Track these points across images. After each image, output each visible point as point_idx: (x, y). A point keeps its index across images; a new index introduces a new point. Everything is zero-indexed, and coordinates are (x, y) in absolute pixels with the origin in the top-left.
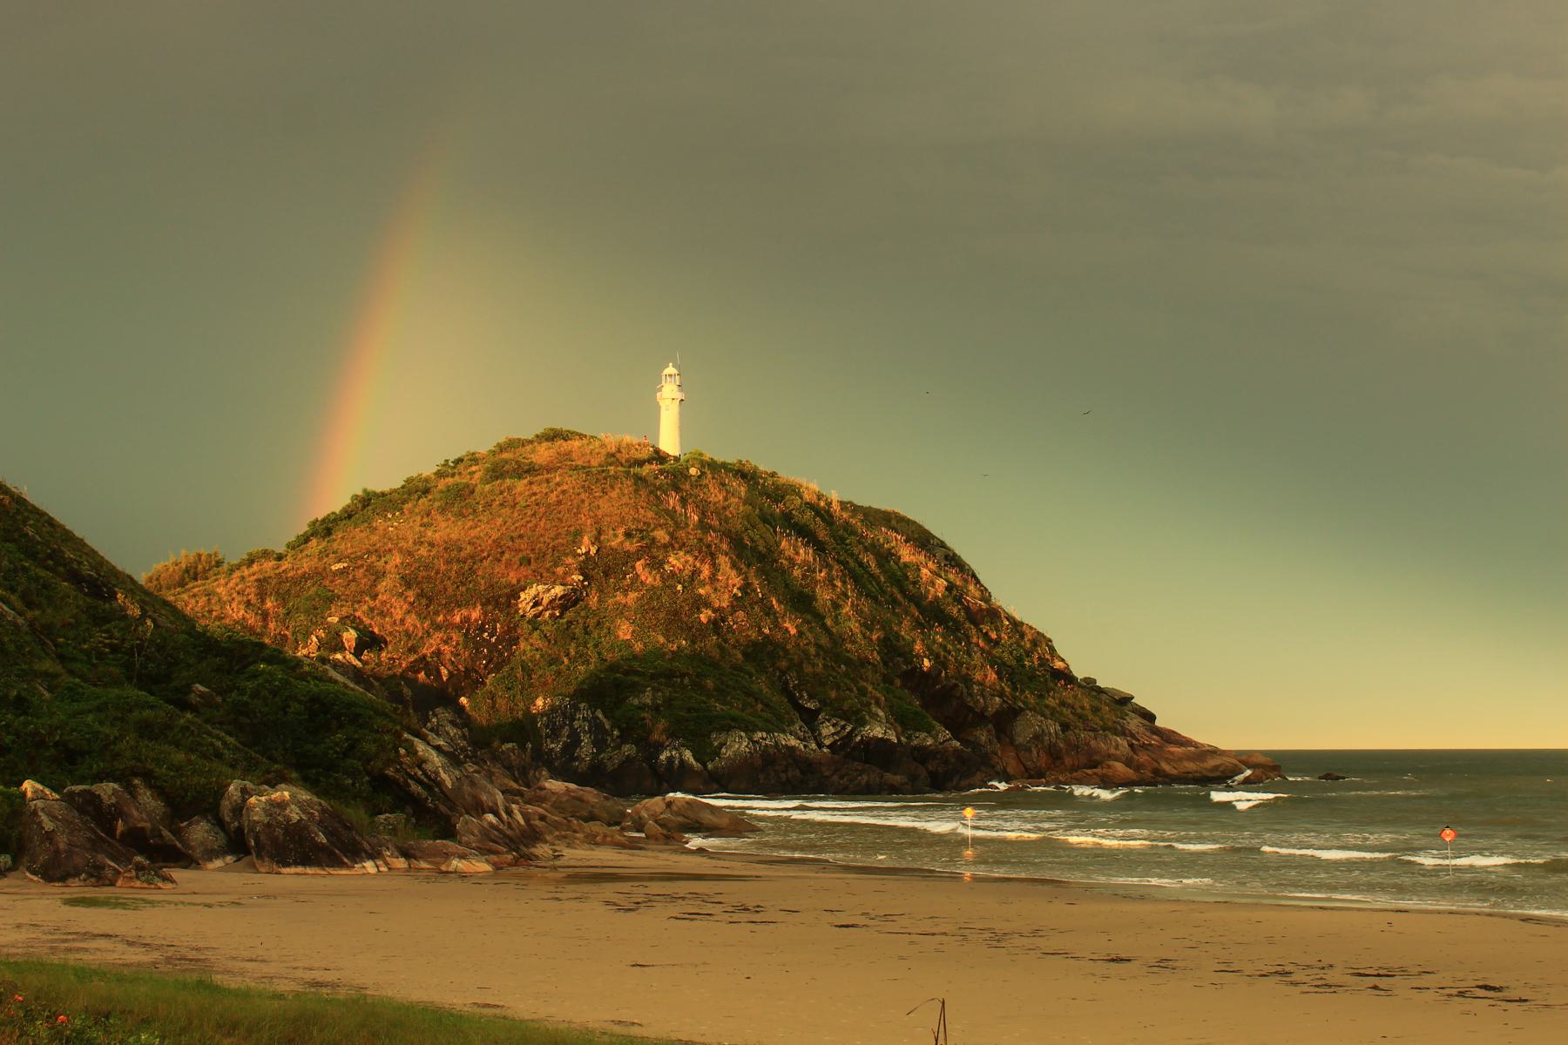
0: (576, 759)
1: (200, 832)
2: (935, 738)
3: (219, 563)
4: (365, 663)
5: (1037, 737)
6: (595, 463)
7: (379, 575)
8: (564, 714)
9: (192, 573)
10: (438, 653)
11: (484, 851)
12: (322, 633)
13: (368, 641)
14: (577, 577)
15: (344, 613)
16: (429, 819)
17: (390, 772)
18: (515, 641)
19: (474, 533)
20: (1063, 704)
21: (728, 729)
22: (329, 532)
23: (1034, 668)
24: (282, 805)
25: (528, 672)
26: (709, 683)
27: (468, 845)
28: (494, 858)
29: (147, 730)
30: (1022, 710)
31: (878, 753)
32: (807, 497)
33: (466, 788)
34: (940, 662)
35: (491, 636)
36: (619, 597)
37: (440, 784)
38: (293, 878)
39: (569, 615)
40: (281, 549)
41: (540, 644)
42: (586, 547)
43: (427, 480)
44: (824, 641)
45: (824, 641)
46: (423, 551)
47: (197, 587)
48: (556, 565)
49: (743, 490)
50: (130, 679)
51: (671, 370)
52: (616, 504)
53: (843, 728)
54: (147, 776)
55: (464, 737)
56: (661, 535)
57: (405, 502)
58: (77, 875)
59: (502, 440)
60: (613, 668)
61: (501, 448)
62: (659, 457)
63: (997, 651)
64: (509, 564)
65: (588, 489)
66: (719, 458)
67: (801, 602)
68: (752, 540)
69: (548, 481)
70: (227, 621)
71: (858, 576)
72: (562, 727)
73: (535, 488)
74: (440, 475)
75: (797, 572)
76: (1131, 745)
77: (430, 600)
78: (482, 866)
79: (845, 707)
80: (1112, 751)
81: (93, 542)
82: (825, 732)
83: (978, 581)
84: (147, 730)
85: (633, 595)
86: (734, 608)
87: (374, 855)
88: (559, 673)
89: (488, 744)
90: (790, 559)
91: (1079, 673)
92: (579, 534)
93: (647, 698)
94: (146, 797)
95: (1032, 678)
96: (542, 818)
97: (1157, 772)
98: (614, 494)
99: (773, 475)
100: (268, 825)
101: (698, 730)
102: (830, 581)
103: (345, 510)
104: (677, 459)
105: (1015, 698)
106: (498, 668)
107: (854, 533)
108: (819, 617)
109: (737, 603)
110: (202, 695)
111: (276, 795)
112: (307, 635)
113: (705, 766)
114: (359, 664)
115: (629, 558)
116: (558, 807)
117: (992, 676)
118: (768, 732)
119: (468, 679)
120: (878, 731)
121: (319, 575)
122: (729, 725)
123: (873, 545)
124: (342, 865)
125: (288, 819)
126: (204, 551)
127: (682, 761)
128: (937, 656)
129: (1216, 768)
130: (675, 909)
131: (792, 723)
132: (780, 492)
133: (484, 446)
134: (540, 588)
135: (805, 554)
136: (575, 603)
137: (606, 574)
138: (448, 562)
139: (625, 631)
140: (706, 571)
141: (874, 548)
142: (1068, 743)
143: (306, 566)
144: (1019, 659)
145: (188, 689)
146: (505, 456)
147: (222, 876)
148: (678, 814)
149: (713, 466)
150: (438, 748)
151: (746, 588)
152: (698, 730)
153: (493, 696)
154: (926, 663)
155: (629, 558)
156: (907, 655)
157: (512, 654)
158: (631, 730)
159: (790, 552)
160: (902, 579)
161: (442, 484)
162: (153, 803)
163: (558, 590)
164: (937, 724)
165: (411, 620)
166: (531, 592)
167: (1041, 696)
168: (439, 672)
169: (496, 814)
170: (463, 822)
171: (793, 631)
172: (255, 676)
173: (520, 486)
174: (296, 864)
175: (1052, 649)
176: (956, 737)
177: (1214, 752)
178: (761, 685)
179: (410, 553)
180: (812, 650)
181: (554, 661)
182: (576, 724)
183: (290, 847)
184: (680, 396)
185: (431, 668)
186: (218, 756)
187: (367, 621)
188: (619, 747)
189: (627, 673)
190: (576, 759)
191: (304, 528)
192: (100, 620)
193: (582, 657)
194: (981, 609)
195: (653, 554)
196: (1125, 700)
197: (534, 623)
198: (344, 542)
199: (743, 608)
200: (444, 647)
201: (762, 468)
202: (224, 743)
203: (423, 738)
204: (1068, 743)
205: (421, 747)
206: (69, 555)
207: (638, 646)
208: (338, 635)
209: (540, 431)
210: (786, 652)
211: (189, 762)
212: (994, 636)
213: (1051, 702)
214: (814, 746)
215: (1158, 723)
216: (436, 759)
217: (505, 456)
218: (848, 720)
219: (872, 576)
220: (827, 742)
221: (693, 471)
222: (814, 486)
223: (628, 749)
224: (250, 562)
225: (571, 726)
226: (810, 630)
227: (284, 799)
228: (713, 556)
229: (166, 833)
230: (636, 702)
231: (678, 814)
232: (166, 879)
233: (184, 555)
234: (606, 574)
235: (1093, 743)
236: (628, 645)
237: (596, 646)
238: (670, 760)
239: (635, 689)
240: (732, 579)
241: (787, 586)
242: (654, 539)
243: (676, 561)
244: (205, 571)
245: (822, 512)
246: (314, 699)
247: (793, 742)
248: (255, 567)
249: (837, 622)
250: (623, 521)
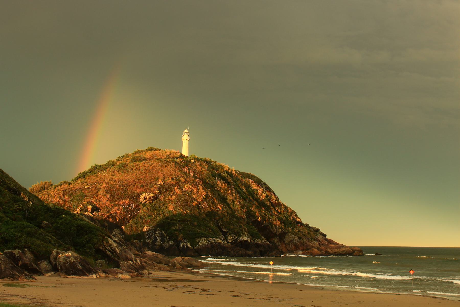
0: (156, 245)
1: (44, 265)
2: (262, 241)
3: (52, 185)
4: (94, 215)
5: (292, 241)
6: (163, 158)
7: (99, 189)
8: (152, 232)
9: (43, 188)
10: (116, 213)
11: (128, 272)
12: (81, 206)
13: (95, 209)
14: (157, 191)
15: (88, 200)
16: (112, 262)
17: (101, 248)
18: (139, 210)
19: (127, 178)
20: (299, 231)
21: (200, 237)
22: (84, 176)
23: (291, 221)
24: (69, 257)
25: (142, 219)
26: (196, 223)
27: (123, 270)
28: (131, 274)
29: (29, 234)
30: (287, 233)
31: (244, 245)
32: (225, 169)
33: (123, 253)
34: (264, 218)
35: (132, 208)
36: (170, 197)
37: (116, 252)
38: (72, 279)
39: (155, 202)
40: (70, 181)
41: (146, 211)
42: (160, 182)
43: (114, 162)
44: (230, 211)
45: (230, 211)
46: (112, 183)
47: (45, 192)
48: (151, 188)
49: (207, 167)
50: (24, 219)
51: (186, 131)
52: (170, 170)
53: (235, 237)
54: (29, 248)
55: (123, 238)
56: (182, 179)
57: (107, 168)
58: (7, 277)
59: (136, 150)
60: (167, 218)
61: (136, 153)
62: (182, 156)
63: (280, 215)
64: (137, 187)
65: (161, 165)
66: (200, 157)
67: (223, 200)
68: (209, 181)
69: (149, 163)
70: (54, 202)
71: (240, 192)
72: (152, 235)
73: (145, 165)
74: (118, 160)
75: (222, 191)
76: (319, 244)
77: (114, 197)
78: (127, 276)
79: (236, 231)
80: (314, 245)
81: (14, 178)
82: (229, 238)
83: (275, 195)
84: (29, 234)
85: (173, 197)
86: (203, 201)
87: (96, 273)
88: (151, 219)
89: (130, 240)
90: (220, 187)
91: (304, 222)
92: (158, 178)
93: (177, 227)
94: (28, 254)
95: (290, 223)
96: (146, 262)
97: (327, 252)
98: (169, 167)
99: (215, 162)
100: (64, 263)
101: (192, 237)
102: (232, 194)
103: (89, 170)
104: (187, 157)
105: (285, 229)
106: (133, 218)
107: (239, 180)
108: (228, 205)
109: (204, 200)
110: (46, 224)
111: (67, 254)
112: (77, 207)
113: (194, 248)
114: (92, 216)
115: (173, 186)
116: (150, 259)
117: (279, 223)
118: (213, 238)
119: (124, 221)
120: (245, 238)
121: (81, 189)
122: (201, 236)
123: (244, 184)
124: (86, 275)
125: (70, 261)
126: (47, 182)
127: (187, 246)
128: (263, 217)
129: (344, 251)
130: (185, 290)
131: (220, 235)
132: (217, 167)
133: (130, 153)
134: (146, 194)
135: (224, 186)
136: (156, 199)
137: (166, 191)
138: (119, 186)
139: (171, 207)
140: (195, 190)
141: (245, 184)
142: (300, 242)
143: (77, 186)
144: (287, 218)
145: (42, 222)
146: (137, 155)
147: (50, 278)
148: (185, 262)
149: (198, 159)
150: (115, 241)
151: (207, 195)
152: (192, 237)
153: (131, 226)
154: (259, 218)
155: (173, 186)
156: (254, 216)
157: (138, 213)
158: (172, 237)
159: (220, 185)
160: (252, 193)
161: (118, 163)
162: (30, 256)
163: (152, 195)
164: (263, 237)
165: (108, 203)
167: (293, 229)
168: (116, 218)
169: (132, 261)
170: (123, 263)
171: (220, 208)
172: (62, 219)
173: (141, 164)
174: (72, 275)
175: (296, 215)
176: (268, 240)
177: (343, 246)
178: (211, 224)
179: (108, 183)
180: (226, 214)
181: (150, 216)
182: (156, 235)
183: (71, 270)
184: (189, 138)
185: (114, 218)
186: (50, 242)
187: (95, 203)
188: (168, 242)
189: (171, 220)
190: (156, 245)
191: (77, 175)
192: (16, 201)
193: (158, 215)
194: (276, 203)
196: (318, 230)
197: (144, 204)
198: (88, 179)
199: (206, 201)
200: (118, 211)
201: (212, 160)
202: (52, 238)
203: (111, 238)
204: (300, 242)
205: (110, 241)
206: (7, 182)
207: (175, 212)
208: (86, 207)
209: (147, 148)
210: (218, 214)
211: (41, 244)
212: (279, 211)
213: (296, 231)
214: (226, 242)
215: (327, 237)
216: (115, 244)
217: (137, 155)
218: (236, 235)
219: (244, 193)
220: (230, 241)
221: (192, 161)
222: (228, 166)
223: (171, 242)
224: (61, 185)
225: (154, 235)
226: (226, 208)
227: (69, 255)
228: (197, 185)
229: (34, 265)
230: (174, 228)
231: (185, 262)
232: (34, 279)
233: (41, 183)
234: (166, 191)
235: (308, 243)
236: (172, 211)
237: (162, 212)
238: (184, 246)
239: (174, 224)
240: (203, 193)
241: (219, 195)
242: (180, 180)
243: (186, 187)
244: (47, 187)
245: (230, 174)
246: (79, 226)
247: (220, 241)
248: (62, 186)
249: (233, 206)
250: (171, 175)
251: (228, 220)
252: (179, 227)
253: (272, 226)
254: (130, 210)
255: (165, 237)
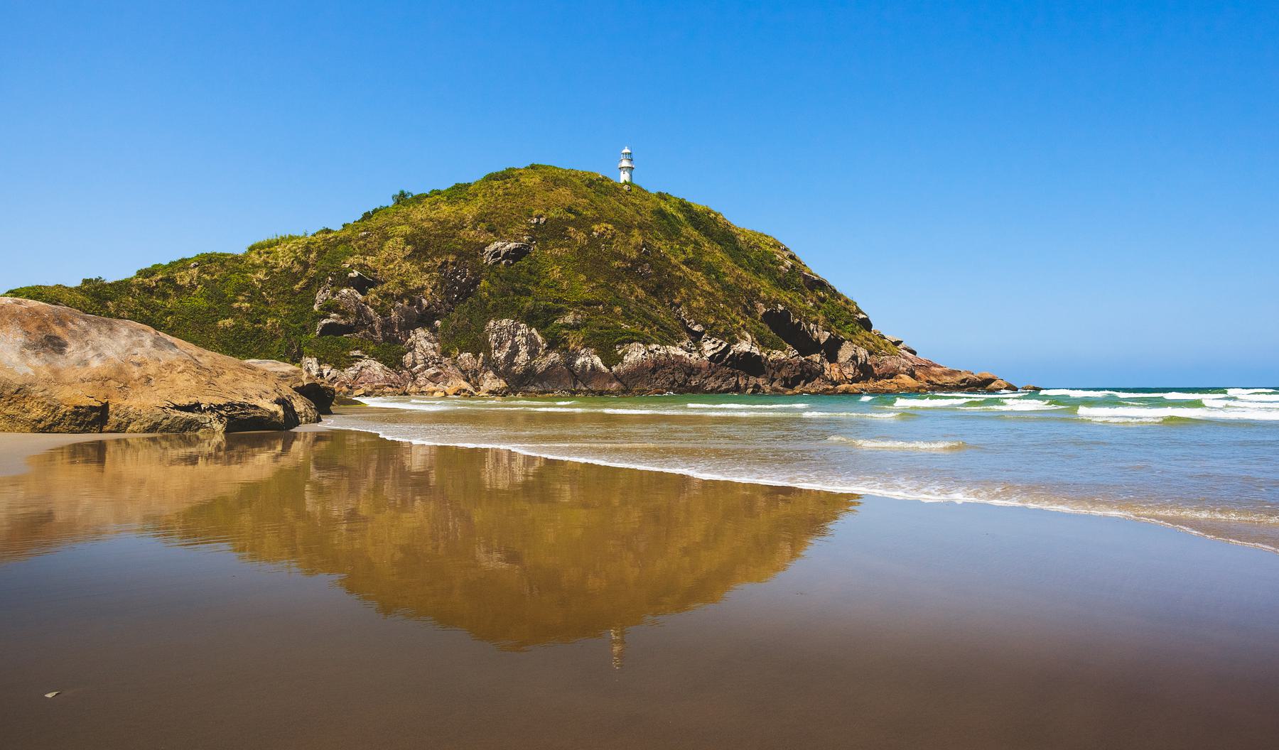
55: (434, 348)
93: (569, 319)
101: (608, 347)
118: (662, 344)
120: (744, 346)
127: (593, 365)
131: (681, 339)
134: (499, 244)
163: (512, 245)
166: (492, 247)
188: (546, 355)
189: (556, 301)
195: (583, 223)
220: (709, 355)
238: (584, 365)
239: (561, 312)
243: (597, 228)
247: (680, 352)
251: (702, 304)
252: (575, 319)
253: (808, 325)
254: (457, 283)
255: (537, 344)
